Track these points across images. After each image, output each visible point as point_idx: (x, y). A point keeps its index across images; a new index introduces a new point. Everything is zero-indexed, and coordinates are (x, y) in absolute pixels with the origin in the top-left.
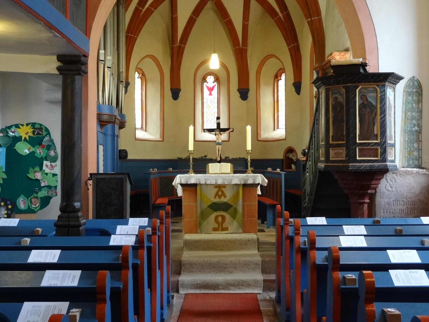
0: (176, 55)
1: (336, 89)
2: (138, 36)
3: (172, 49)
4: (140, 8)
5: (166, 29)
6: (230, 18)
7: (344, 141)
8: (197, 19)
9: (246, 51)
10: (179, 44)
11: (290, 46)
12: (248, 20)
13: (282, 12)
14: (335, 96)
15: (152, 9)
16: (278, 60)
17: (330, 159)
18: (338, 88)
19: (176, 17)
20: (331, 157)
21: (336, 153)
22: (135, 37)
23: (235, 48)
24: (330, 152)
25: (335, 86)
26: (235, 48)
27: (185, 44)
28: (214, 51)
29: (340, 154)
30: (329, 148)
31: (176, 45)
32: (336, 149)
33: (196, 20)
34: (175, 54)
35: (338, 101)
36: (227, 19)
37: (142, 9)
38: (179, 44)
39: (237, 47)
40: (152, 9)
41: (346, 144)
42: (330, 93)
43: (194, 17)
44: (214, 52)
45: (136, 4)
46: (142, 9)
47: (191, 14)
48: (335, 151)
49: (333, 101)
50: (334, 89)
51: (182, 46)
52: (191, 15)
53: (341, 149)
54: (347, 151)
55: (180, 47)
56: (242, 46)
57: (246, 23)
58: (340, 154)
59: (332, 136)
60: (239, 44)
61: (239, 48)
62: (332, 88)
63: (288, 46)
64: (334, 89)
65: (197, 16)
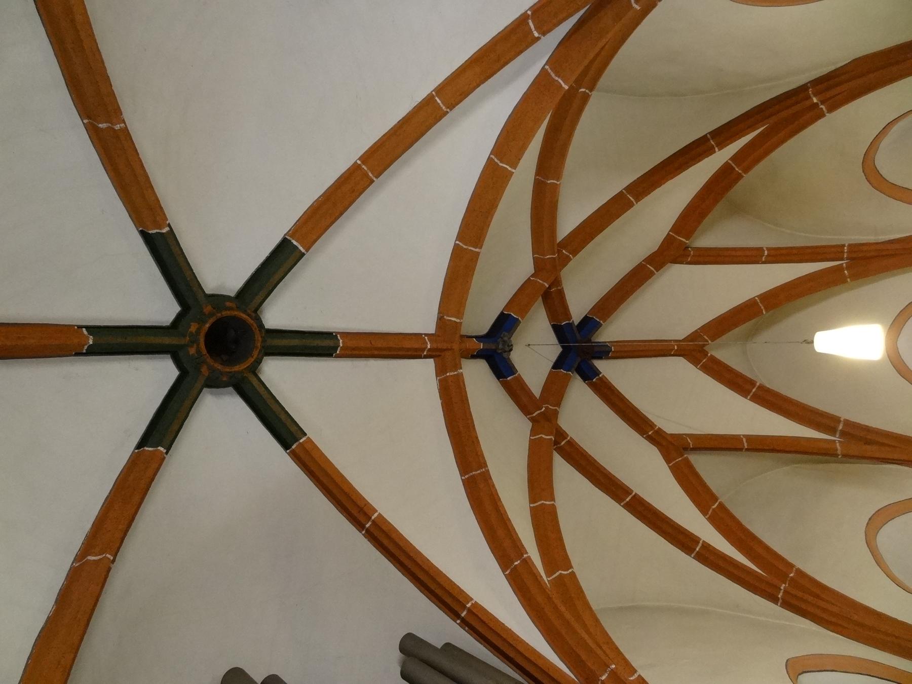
0: (868, 447)
2: (791, 566)
3: (849, 457)
4: (697, 549)
5: (795, 465)
6: (756, 298)
8: (758, 384)
9: (855, 248)
10: (837, 436)
11: (822, 109)
12: (760, 250)
13: (709, 151)
15: (714, 510)
16: (885, 143)
19: (749, 438)
22: (791, 575)
23: (849, 280)
26: (849, 280)
27: (837, 420)
28: (805, 345)
31: (839, 448)
33: (762, 387)
34: (870, 450)
36: (761, 305)
37: (700, 545)
38: (837, 436)
39: (846, 272)
40: (714, 507)
43: (754, 390)
44: (808, 343)
45: (688, 557)
46: (700, 545)
47: (746, 398)
51: (840, 427)
52: (750, 400)
55: (843, 434)
56: (842, 259)
57: (766, 253)
60: (839, 269)
61: (848, 268)
63: (821, 115)
65: (752, 383)
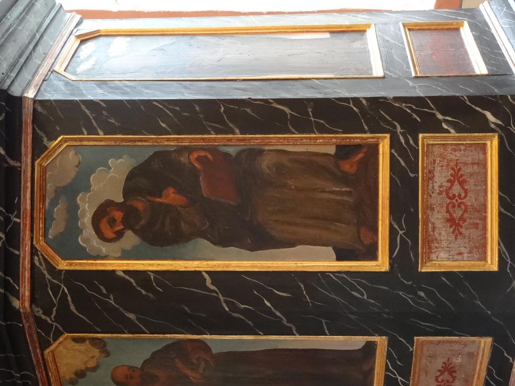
1: (48, 220)
7: (374, 149)
14: (89, 231)
17: (495, 268)
18: (43, 198)
20: (476, 266)
21: (451, 221)
24: (445, 274)
25: (25, 223)
29: (462, 184)
30: (421, 272)
32: (426, 222)
35: (120, 199)
41: (399, 129)
42: (63, 265)
48: (439, 224)
49: (115, 247)
50: (45, 235)
53: (430, 176)
54: (440, 117)
58: (456, 189)
59: (339, 258)
62: (34, 251)
64: (45, 235)
